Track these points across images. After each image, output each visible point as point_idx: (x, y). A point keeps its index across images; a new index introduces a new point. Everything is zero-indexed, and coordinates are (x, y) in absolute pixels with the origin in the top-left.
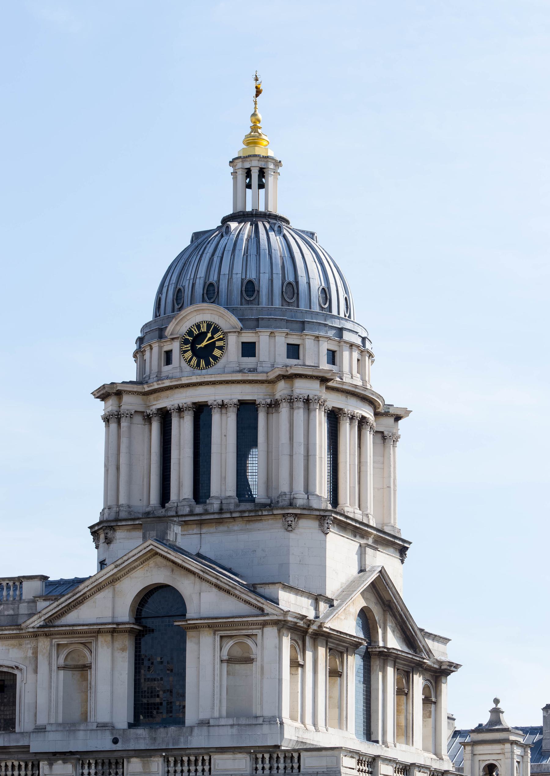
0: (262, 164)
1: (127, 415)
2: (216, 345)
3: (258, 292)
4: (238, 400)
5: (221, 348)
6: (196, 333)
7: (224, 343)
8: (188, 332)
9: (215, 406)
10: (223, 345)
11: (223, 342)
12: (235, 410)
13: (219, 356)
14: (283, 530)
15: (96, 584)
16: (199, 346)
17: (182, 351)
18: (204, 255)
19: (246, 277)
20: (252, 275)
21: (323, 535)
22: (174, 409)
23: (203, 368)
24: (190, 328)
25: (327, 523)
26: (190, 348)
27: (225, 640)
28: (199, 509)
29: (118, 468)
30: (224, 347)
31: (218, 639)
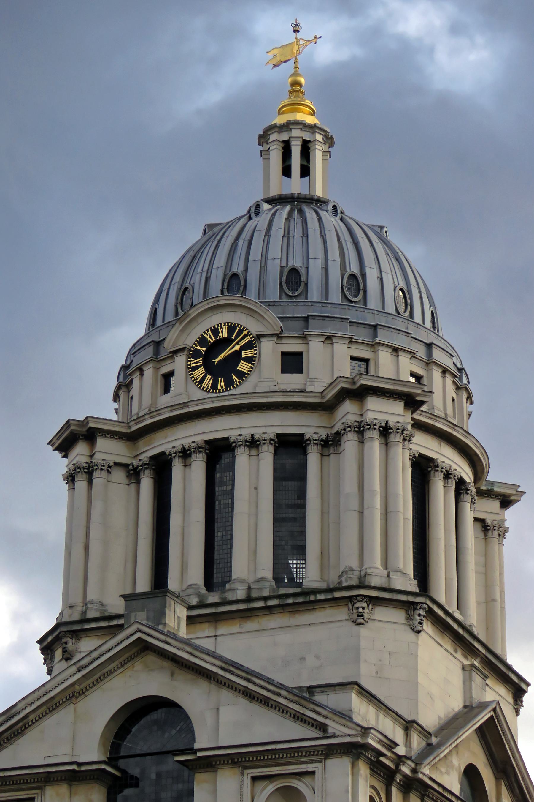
0: (307, 136)
1: (103, 467)
2: (243, 356)
3: (306, 284)
4: (276, 434)
5: (249, 360)
6: (212, 341)
7: (255, 352)
8: (198, 340)
9: (241, 443)
10: (253, 355)
11: (253, 350)
12: (272, 449)
13: (246, 372)
14: (349, 623)
15: (45, 699)
16: (217, 360)
17: (189, 368)
18: (223, 240)
19: (287, 264)
20: (297, 262)
21: (412, 636)
22: (175, 453)
23: (221, 391)
24: (202, 335)
25: (419, 615)
26: (201, 364)
27: (260, 785)
28: (213, 598)
29: (87, 548)
30: (255, 357)
31: (248, 781)
